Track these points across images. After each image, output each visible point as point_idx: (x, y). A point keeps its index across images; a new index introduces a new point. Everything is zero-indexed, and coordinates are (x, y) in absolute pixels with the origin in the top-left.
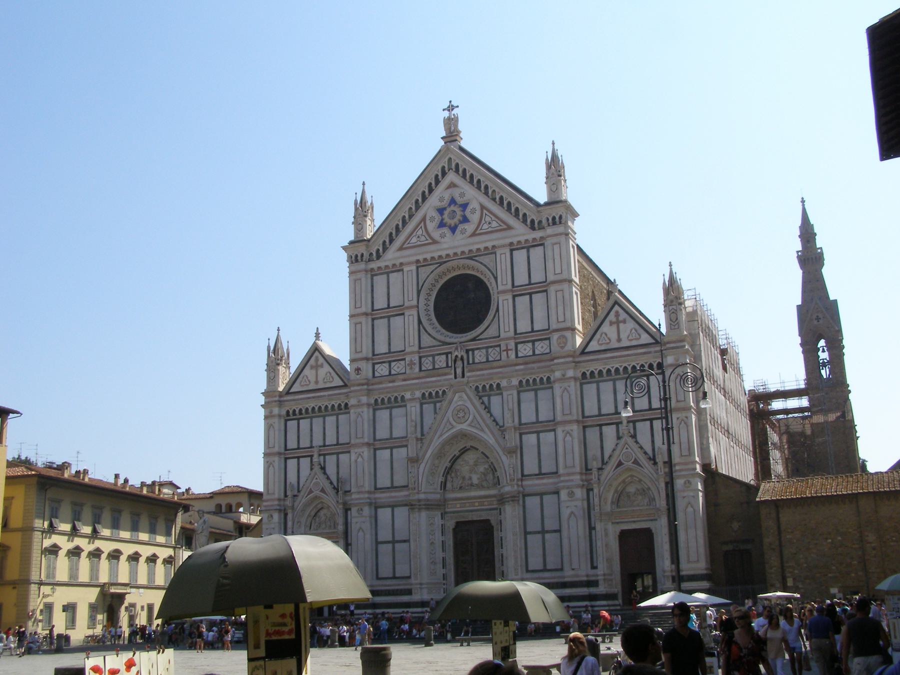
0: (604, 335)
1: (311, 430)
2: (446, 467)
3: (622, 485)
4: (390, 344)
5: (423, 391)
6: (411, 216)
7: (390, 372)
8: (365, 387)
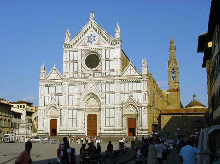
6: (81, 38)
7: (73, 76)
8: (67, 80)
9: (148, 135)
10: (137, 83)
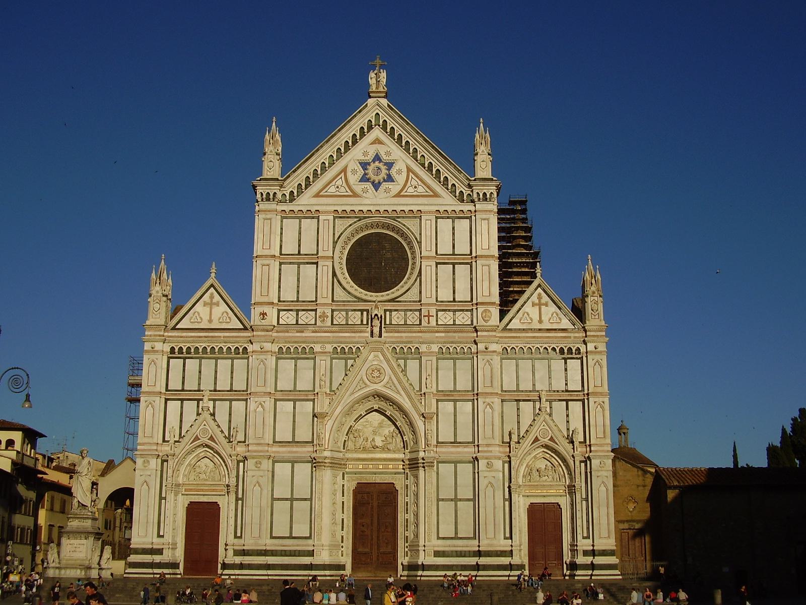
0: (526, 314)
1: (200, 372)
3: (533, 459)
5: (335, 345)
6: (332, 164)
7: (297, 321)
9: (617, 572)
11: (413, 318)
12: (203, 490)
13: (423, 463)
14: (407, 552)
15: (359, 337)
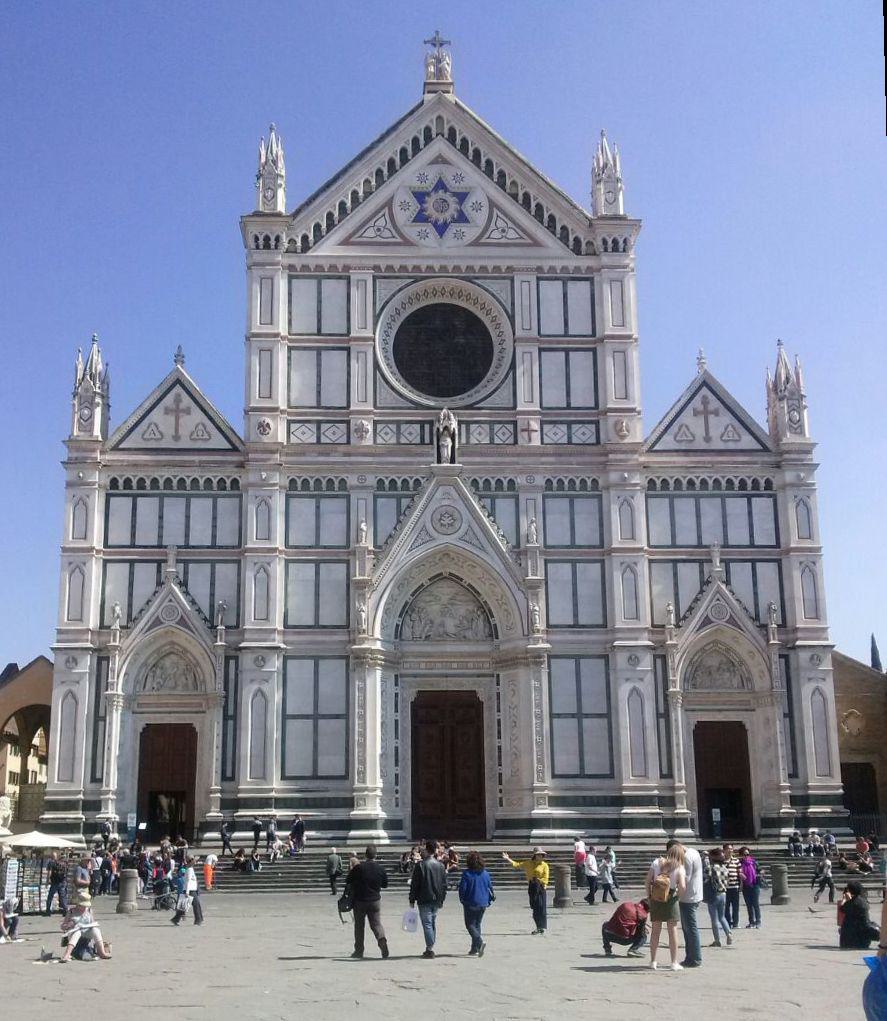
1: (161, 517)
2: (406, 603)
4: (319, 393)
7: (319, 438)
10: (749, 498)
11: (504, 434)
12: (167, 705)
13: (527, 658)
14: (501, 799)
15: (419, 463)
